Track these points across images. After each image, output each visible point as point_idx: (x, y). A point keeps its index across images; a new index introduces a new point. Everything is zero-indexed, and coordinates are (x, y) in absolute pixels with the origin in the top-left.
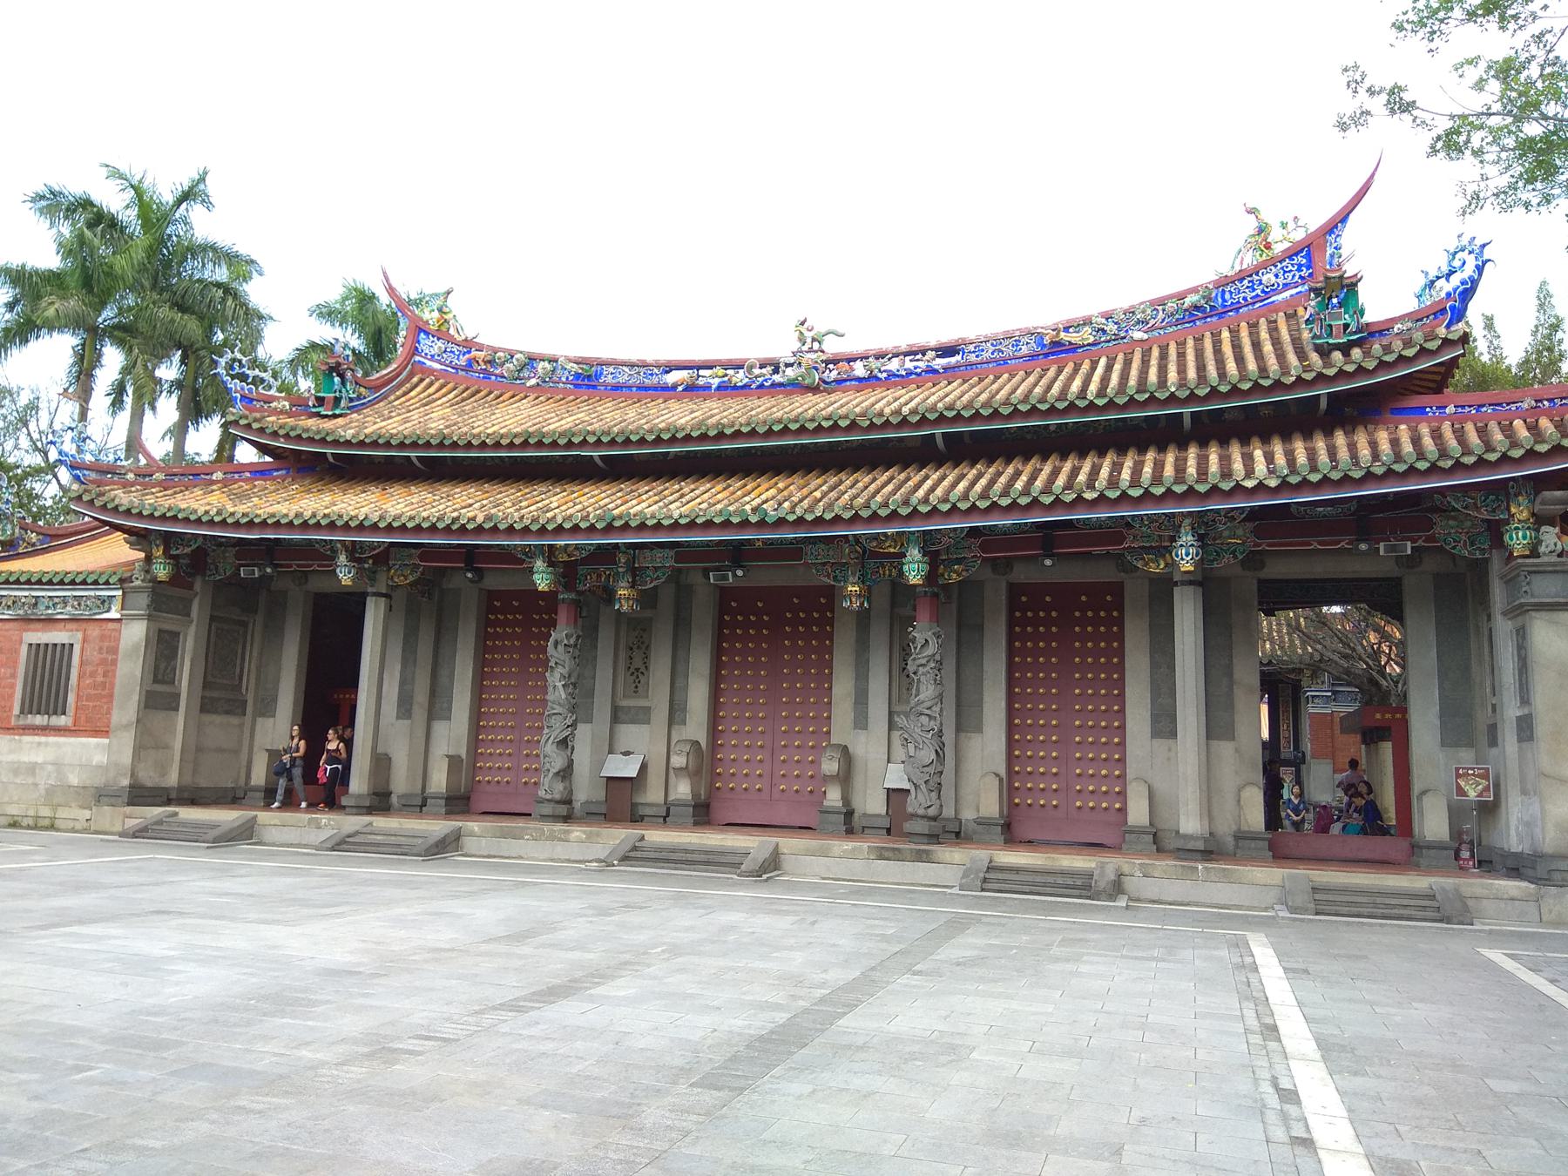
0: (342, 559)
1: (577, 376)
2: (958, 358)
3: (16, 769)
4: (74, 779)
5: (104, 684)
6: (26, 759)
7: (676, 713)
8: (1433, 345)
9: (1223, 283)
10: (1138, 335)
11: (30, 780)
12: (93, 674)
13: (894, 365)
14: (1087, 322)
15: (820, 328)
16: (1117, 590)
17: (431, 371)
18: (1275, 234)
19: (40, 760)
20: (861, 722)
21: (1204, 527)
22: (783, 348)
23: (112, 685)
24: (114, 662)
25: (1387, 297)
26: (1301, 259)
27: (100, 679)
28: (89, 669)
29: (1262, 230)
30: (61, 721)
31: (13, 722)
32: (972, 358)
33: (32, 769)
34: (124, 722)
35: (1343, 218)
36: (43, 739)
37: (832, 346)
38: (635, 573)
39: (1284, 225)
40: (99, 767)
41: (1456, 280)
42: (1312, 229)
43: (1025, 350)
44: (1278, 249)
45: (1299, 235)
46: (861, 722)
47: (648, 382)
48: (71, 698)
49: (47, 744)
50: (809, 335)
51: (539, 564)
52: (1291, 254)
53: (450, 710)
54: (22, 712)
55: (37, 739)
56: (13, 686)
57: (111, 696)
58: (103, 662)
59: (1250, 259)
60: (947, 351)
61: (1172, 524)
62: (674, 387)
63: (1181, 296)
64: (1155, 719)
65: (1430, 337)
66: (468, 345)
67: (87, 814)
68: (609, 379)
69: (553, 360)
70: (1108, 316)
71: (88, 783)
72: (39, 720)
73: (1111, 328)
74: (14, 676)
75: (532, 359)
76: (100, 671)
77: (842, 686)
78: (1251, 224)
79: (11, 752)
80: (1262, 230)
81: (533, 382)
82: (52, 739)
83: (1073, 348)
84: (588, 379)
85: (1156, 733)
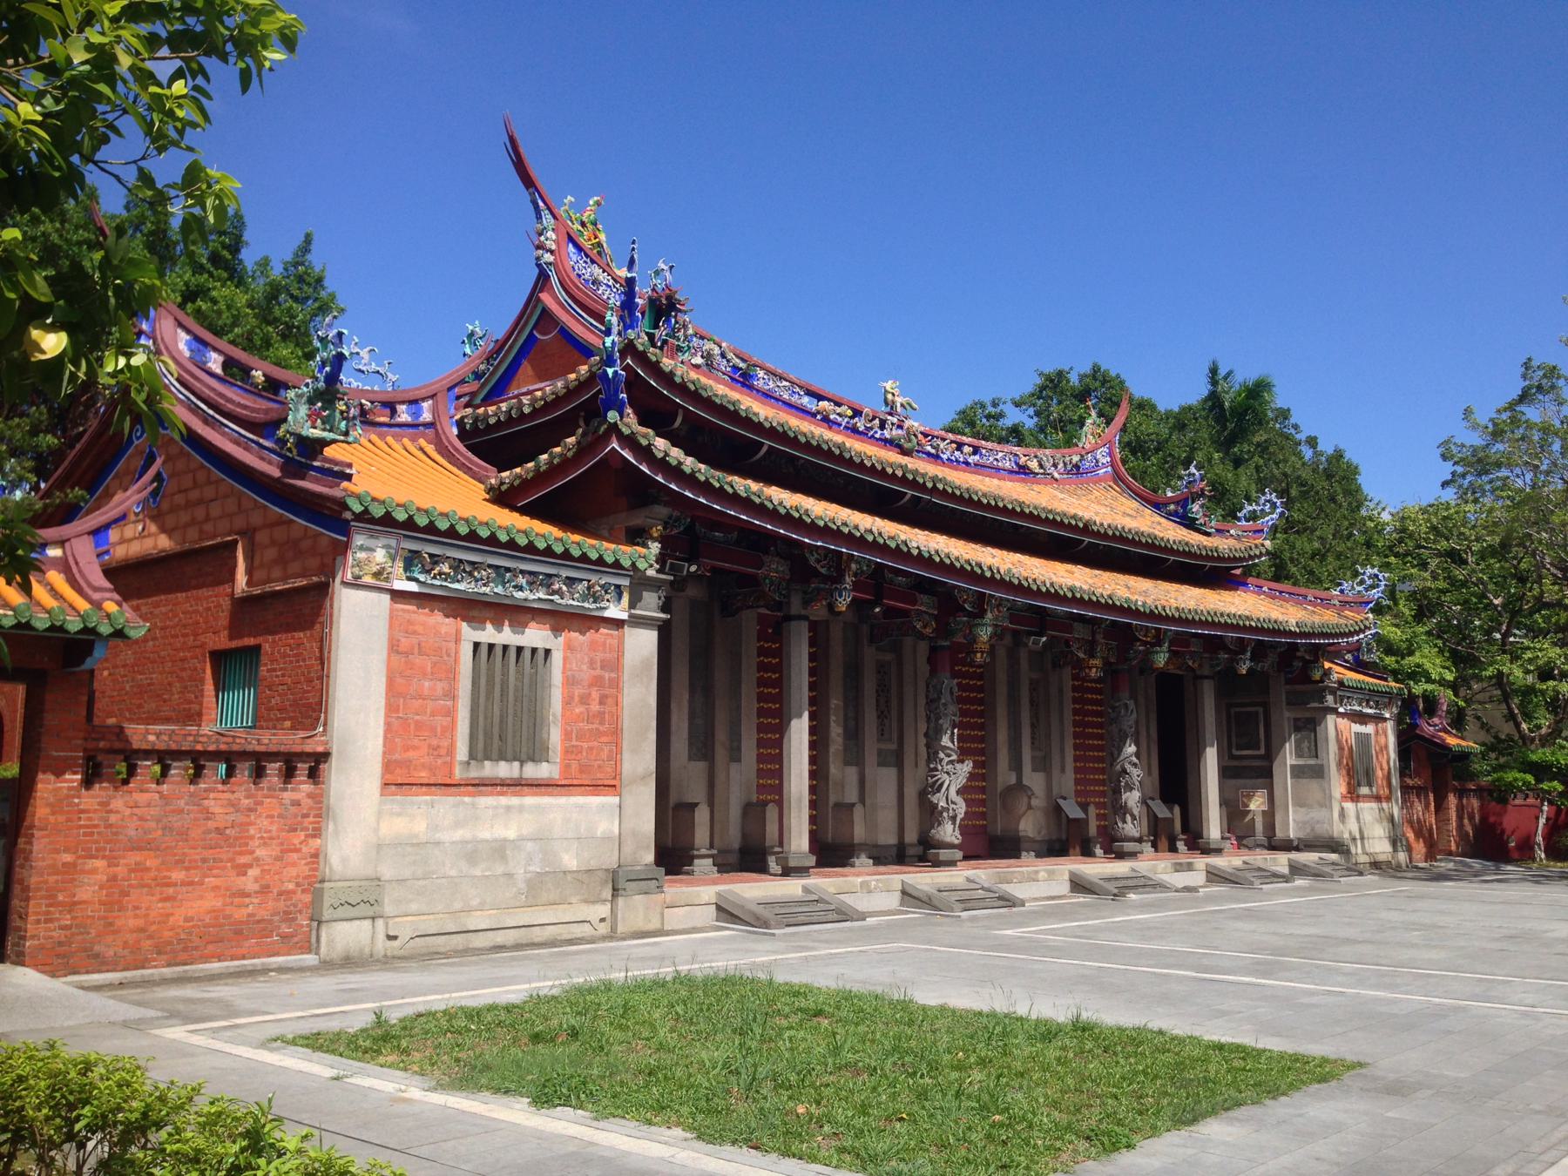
3: (472, 852)
4: (570, 861)
5: (601, 714)
6: (486, 835)
11: (500, 869)
12: (585, 700)
19: (511, 834)
23: (617, 719)
24: (616, 684)
27: (595, 707)
28: (577, 692)
30: (542, 771)
31: (458, 774)
33: (500, 849)
34: (640, 770)
36: (515, 801)
40: (606, 839)
48: (555, 737)
49: (521, 809)
54: (472, 756)
55: (503, 800)
56: (451, 713)
57: (616, 732)
58: (597, 682)
67: (604, 910)
71: (594, 864)
72: (505, 770)
74: (452, 695)
76: (595, 695)
79: (457, 825)
82: (530, 801)
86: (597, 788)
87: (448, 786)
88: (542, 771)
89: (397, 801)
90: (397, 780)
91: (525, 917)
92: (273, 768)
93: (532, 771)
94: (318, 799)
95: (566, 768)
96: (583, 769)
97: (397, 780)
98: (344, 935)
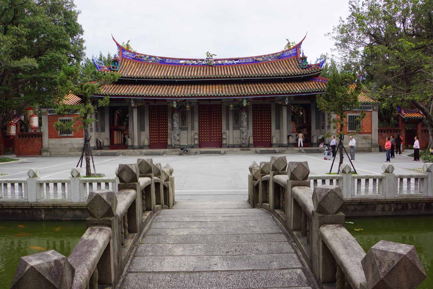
0: (132, 101)
1: (160, 61)
2: (238, 61)
4: (76, 146)
7: (193, 128)
8: (318, 70)
9: (283, 52)
10: (270, 60)
13: (226, 62)
14: (261, 56)
15: (212, 54)
16: (270, 105)
17: (127, 59)
18: (291, 44)
20: (228, 128)
21: (289, 98)
22: (205, 57)
25: (312, 60)
26: (295, 49)
29: (289, 43)
30: (71, 135)
32: (241, 62)
33: (65, 145)
35: (301, 43)
37: (214, 57)
38: (190, 103)
39: (292, 43)
41: (321, 61)
42: (297, 44)
43: (250, 61)
44: (292, 47)
45: (295, 45)
46: (228, 128)
47: (174, 63)
50: (209, 55)
51: (175, 102)
52: (293, 48)
53: (144, 129)
59: (287, 49)
60: (236, 60)
61: (285, 98)
62: (182, 64)
63: (277, 54)
64: (276, 126)
65: (318, 69)
66: (135, 53)
68: (168, 62)
69: (155, 57)
70: (265, 56)
72: (65, 135)
73: (265, 58)
75: (150, 57)
77: (224, 123)
78: (287, 42)
80: (289, 43)
81: (151, 62)
82: (69, 139)
83: (259, 61)
84: (163, 62)
85: (276, 129)
86: (80, 137)
87: (58, 137)
88: (71, 135)
89: (50, 140)
90: (50, 137)
91: (69, 153)
92: (37, 136)
93: (69, 135)
94: (42, 139)
95: (74, 135)
96: (77, 135)
97: (50, 137)
98: (44, 154)
